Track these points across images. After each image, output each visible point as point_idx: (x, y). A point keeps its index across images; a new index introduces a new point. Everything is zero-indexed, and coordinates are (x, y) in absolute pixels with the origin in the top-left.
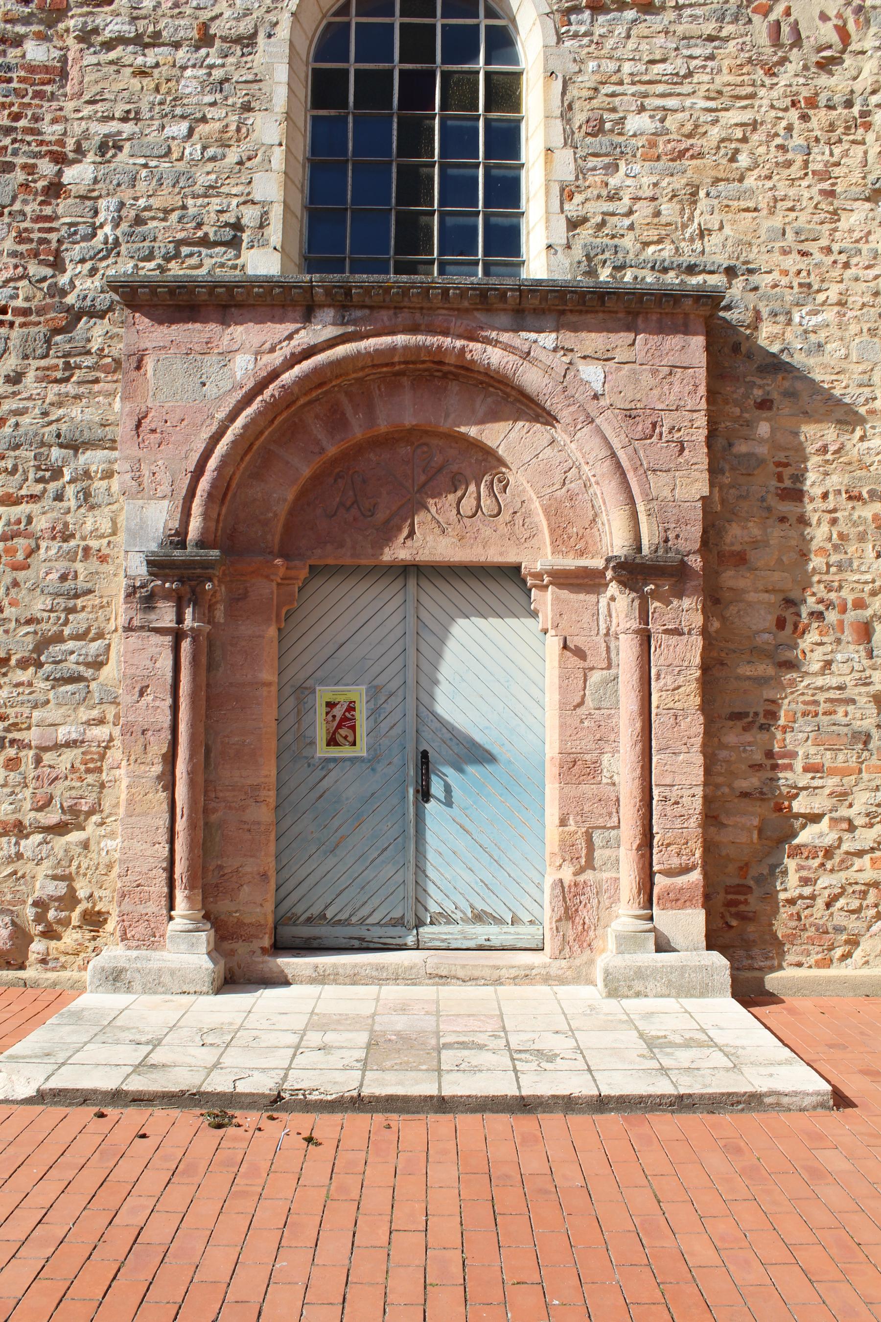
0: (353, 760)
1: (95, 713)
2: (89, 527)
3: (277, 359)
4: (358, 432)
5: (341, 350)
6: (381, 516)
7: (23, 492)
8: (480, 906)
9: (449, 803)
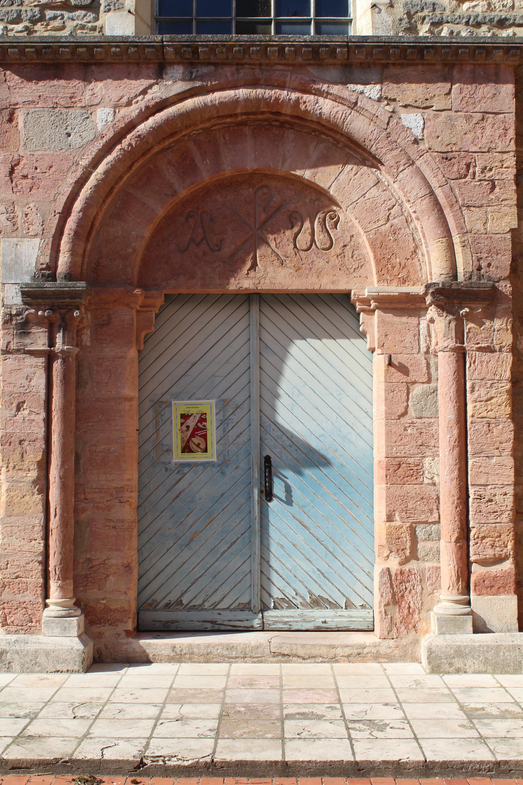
0: (205, 465)
3: (133, 111)
5: (190, 103)
6: (227, 250)
8: (318, 592)
9: (289, 501)
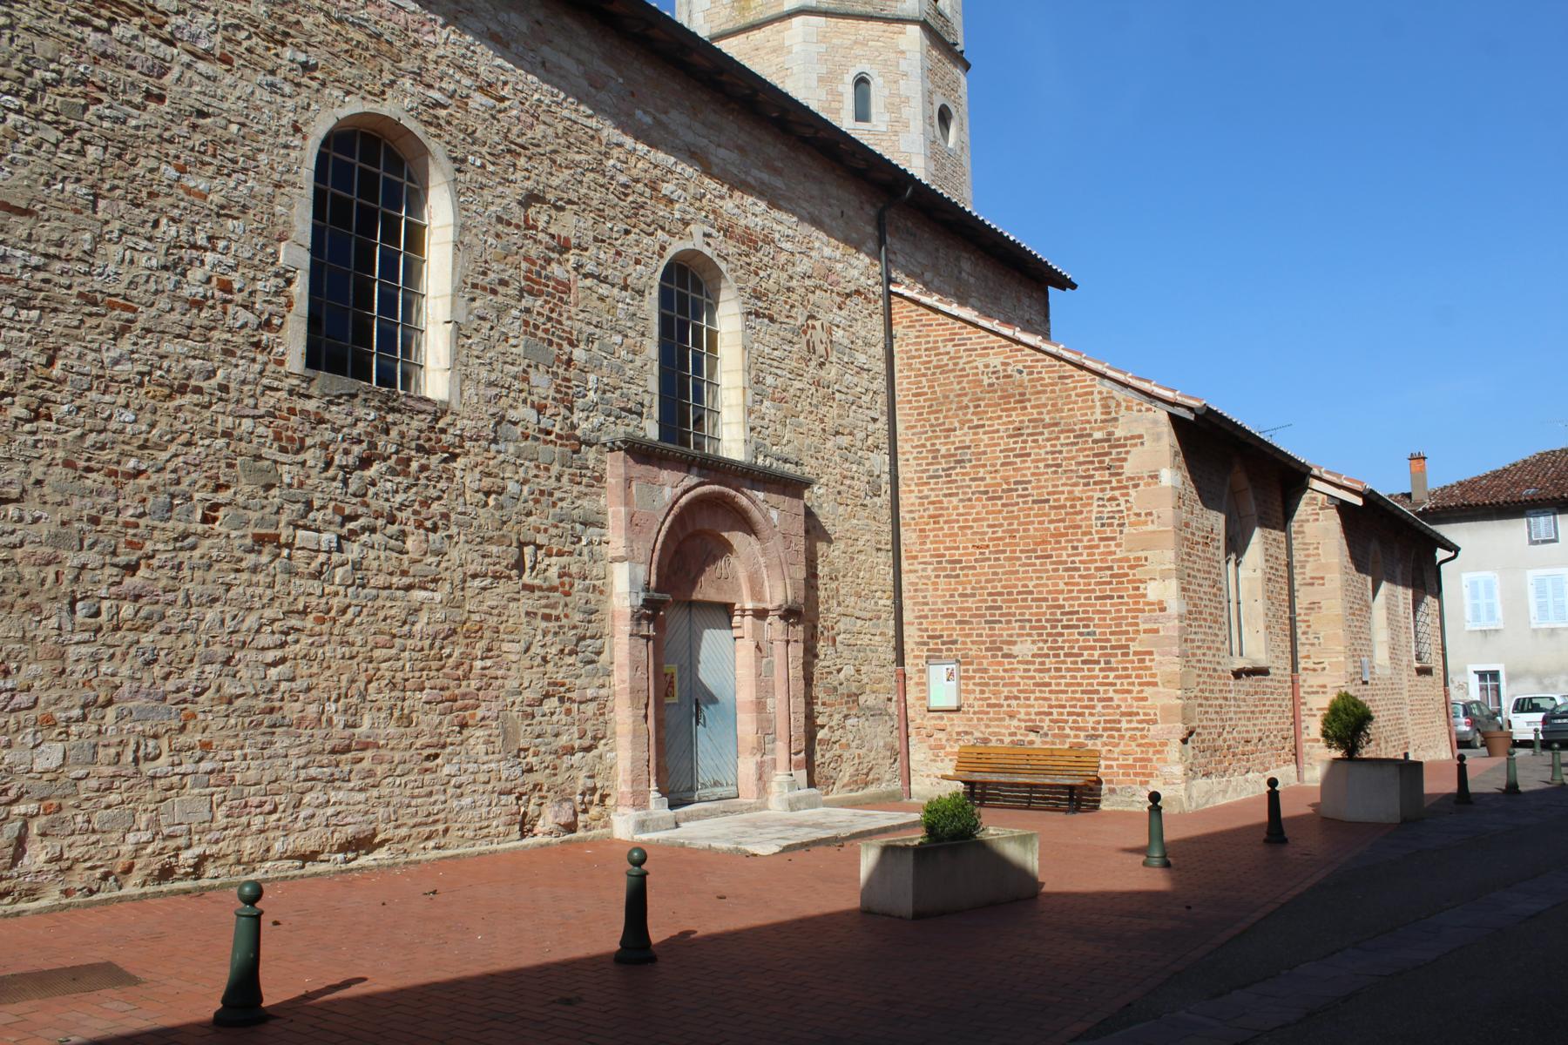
1: (601, 681)
2: (594, 573)
3: (679, 491)
4: (690, 530)
6: (693, 575)
7: (566, 549)
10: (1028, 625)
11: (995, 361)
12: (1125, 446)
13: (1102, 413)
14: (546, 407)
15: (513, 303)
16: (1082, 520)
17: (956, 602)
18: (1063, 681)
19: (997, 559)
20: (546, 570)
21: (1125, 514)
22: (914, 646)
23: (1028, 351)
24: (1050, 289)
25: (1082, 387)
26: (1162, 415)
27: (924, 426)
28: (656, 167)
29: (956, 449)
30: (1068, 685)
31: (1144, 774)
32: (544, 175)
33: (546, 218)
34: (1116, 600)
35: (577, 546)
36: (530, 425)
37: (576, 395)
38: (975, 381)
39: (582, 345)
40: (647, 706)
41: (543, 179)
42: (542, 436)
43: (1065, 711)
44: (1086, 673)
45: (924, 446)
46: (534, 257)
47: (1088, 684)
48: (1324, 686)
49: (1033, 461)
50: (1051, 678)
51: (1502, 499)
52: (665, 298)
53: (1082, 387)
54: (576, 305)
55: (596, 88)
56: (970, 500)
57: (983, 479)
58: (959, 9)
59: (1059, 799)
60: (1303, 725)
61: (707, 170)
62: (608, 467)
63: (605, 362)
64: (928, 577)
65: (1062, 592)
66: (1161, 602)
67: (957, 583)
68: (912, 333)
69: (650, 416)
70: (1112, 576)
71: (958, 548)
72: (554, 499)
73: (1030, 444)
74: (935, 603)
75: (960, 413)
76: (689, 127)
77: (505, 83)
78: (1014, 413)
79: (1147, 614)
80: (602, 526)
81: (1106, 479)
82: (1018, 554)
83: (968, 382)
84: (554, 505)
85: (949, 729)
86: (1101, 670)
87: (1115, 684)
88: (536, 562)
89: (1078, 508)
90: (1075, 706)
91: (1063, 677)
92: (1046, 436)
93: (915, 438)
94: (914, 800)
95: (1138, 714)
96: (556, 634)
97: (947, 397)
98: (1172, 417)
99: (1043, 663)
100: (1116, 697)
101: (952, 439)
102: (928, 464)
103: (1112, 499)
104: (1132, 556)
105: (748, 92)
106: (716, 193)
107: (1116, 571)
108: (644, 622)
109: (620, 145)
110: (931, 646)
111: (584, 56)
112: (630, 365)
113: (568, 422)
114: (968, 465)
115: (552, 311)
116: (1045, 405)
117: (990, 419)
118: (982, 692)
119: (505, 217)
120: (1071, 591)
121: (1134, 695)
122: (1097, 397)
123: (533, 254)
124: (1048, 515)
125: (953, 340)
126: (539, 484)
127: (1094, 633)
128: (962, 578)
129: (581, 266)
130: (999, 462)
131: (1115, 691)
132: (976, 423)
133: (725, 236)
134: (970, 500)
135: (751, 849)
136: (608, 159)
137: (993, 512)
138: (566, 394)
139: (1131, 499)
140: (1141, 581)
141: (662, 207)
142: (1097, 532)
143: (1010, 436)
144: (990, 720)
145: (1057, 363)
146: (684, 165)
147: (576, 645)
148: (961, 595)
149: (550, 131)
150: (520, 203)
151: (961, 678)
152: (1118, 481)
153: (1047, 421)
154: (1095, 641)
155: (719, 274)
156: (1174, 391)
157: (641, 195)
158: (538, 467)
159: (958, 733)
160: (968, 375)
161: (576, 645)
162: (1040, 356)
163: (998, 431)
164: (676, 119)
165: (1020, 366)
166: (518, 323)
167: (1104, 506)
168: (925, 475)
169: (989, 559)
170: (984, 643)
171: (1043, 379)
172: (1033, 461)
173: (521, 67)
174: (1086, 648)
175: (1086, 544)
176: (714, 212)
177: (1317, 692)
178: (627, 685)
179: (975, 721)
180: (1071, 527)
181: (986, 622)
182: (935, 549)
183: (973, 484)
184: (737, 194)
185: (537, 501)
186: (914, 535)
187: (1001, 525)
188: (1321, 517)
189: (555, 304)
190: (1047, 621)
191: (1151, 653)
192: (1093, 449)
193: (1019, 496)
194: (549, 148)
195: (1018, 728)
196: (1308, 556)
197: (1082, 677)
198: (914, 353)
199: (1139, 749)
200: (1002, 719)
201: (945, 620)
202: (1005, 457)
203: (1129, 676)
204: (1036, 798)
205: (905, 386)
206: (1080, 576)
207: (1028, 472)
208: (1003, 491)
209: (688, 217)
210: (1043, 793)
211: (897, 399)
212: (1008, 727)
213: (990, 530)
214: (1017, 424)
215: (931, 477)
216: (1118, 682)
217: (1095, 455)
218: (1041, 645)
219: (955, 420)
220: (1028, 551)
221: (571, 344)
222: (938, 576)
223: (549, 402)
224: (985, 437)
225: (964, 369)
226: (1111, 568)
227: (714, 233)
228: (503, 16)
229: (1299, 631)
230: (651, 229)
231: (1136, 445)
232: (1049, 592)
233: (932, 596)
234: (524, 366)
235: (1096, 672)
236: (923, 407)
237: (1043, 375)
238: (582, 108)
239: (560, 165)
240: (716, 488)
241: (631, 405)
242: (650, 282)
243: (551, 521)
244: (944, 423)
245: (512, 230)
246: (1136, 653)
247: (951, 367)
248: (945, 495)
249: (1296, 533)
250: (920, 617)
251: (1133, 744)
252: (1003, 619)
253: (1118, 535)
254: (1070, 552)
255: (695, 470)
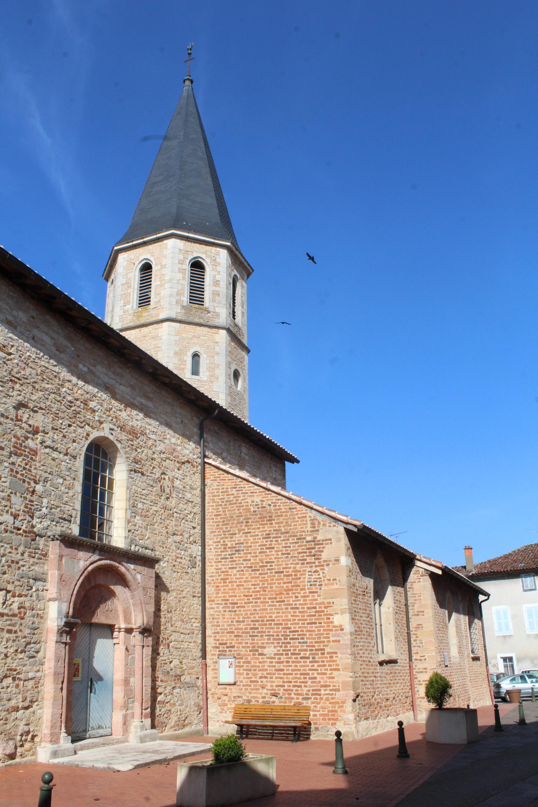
0: (78, 681)
1: (38, 668)
2: (38, 607)
3: (88, 563)
4: (93, 584)
6: (92, 609)
7: (23, 593)
8: (100, 724)
9: (95, 693)
10: (272, 638)
11: (257, 499)
12: (322, 544)
13: (311, 527)
14: (18, 515)
15: (6, 459)
16: (300, 582)
17: (234, 625)
18: (290, 668)
19: (256, 603)
20: (11, 605)
21: (322, 579)
22: (211, 649)
23: (274, 494)
24: (286, 463)
25: (301, 514)
26: (341, 529)
27: (219, 532)
28: (87, 393)
29: (236, 544)
30: (292, 670)
31: (333, 719)
32: (28, 394)
33: (28, 416)
34: (318, 625)
35: (30, 592)
36: (9, 525)
37: (37, 510)
38: (247, 509)
39: (41, 483)
40: (63, 682)
41: (27, 396)
42: (15, 531)
43: (292, 684)
44: (302, 664)
45: (219, 542)
46: (19, 436)
47: (303, 670)
48: (426, 669)
49: (276, 551)
50: (284, 666)
51: (509, 569)
52: (88, 460)
53: (301, 514)
54: (40, 462)
55: (60, 352)
56: (243, 571)
57: (249, 560)
58: (246, 323)
59: (288, 734)
60: (416, 690)
61: (114, 396)
62: (50, 549)
63: (53, 493)
64: (220, 612)
65: (290, 620)
66: (341, 626)
67: (235, 615)
68: (215, 483)
69: (75, 523)
70: (316, 612)
71: (236, 596)
72: (19, 565)
73: (274, 542)
74: (223, 625)
75: (239, 525)
76: (106, 374)
77: (12, 346)
78: (266, 526)
79: (334, 632)
80: (45, 581)
81: (313, 561)
82: (267, 600)
83: (243, 510)
84: (19, 568)
85: (229, 695)
86: (310, 662)
87: (317, 670)
88: (6, 600)
89: (298, 576)
90: (296, 682)
91: (291, 666)
92: (282, 538)
93: (215, 538)
94: (210, 735)
95: (330, 686)
96: (14, 641)
97: (232, 517)
98: (347, 530)
99: (280, 658)
100: (318, 677)
101: (234, 539)
102: (221, 552)
103: (316, 571)
104: (326, 601)
105: (137, 359)
106: (118, 408)
107: (318, 609)
108: (64, 635)
109: (69, 381)
110: (221, 649)
111: (55, 336)
112: (66, 495)
113: (30, 524)
114: (242, 552)
115: (26, 464)
116: (282, 523)
117: (254, 529)
118: (248, 674)
119: (6, 414)
120: (294, 620)
121: (328, 675)
122: (308, 519)
123: (19, 434)
124: (283, 579)
125: (236, 488)
126: (11, 557)
127: (307, 642)
128: (237, 612)
129: (44, 442)
130: (258, 551)
131: (318, 674)
132: (246, 531)
133: (121, 430)
134: (243, 571)
135: (117, 767)
136: (63, 388)
137: (254, 578)
138: (31, 509)
139: (325, 572)
140: (331, 615)
141: (89, 413)
142: (308, 589)
143: (264, 538)
144: (252, 689)
145: (288, 501)
146: (102, 393)
147: (25, 647)
148: (237, 621)
149: (34, 372)
150: (14, 407)
151: (236, 666)
152: (319, 562)
153: (283, 530)
154: (307, 646)
155: (116, 450)
156: (347, 516)
157: (79, 407)
158: (11, 548)
159: (235, 697)
160: (243, 506)
161: (25, 647)
162: (280, 497)
163: (258, 535)
164: (100, 370)
165: (270, 502)
166: (7, 470)
167: (311, 575)
168: (219, 557)
169: (252, 602)
170: (249, 647)
171: (281, 509)
172: (276, 551)
173: (22, 339)
174: (302, 650)
175: (302, 595)
176: (116, 418)
177: (422, 672)
178: (52, 670)
179: (244, 690)
180: (294, 586)
181: (250, 636)
182: (224, 597)
183: (245, 562)
184: (129, 409)
185: (9, 566)
186: (213, 589)
187: (259, 584)
188: (421, 580)
189: (29, 461)
190: (282, 635)
191: (336, 653)
192: (306, 545)
193: (268, 569)
194: (32, 380)
195: (267, 694)
196: (415, 600)
197: (300, 666)
198: (216, 494)
199: (330, 705)
200: (259, 689)
201: (228, 635)
202: (262, 549)
203: (325, 666)
204: (276, 733)
205: (211, 510)
206: (300, 612)
207: (273, 557)
208: (260, 566)
209: (102, 420)
210: (280, 730)
211: (206, 517)
212: (261, 694)
213: (253, 587)
214: (267, 532)
215: (223, 559)
216: (319, 668)
217: (307, 549)
218: (279, 648)
219: (236, 529)
220: (272, 598)
221: (35, 482)
222: (225, 611)
223: (21, 513)
224: (251, 538)
225: (241, 503)
226: (315, 608)
227: (115, 428)
228: (15, 313)
229: (412, 639)
230: (83, 425)
231: (328, 544)
232: (283, 620)
233: (222, 622)
234: (9, 493)
235: (308, 663)
236: (220, 522)
237: (281, 507)
238: (51, 361)
239: (37, 389)
240: (108, 562)
241: (65, 516)
242: (80, 452)
243: (16, 577)
244: (230, 531)
245: (9, 421)
246: (328, 653)
247: (234, 501)
248: (230, 568)
249: (410, 588)
250: (215, 633)
251: (328, 702)
252: (259, 635)
253: (318, 590)
254: (294, 599)
255: (97, 552)
